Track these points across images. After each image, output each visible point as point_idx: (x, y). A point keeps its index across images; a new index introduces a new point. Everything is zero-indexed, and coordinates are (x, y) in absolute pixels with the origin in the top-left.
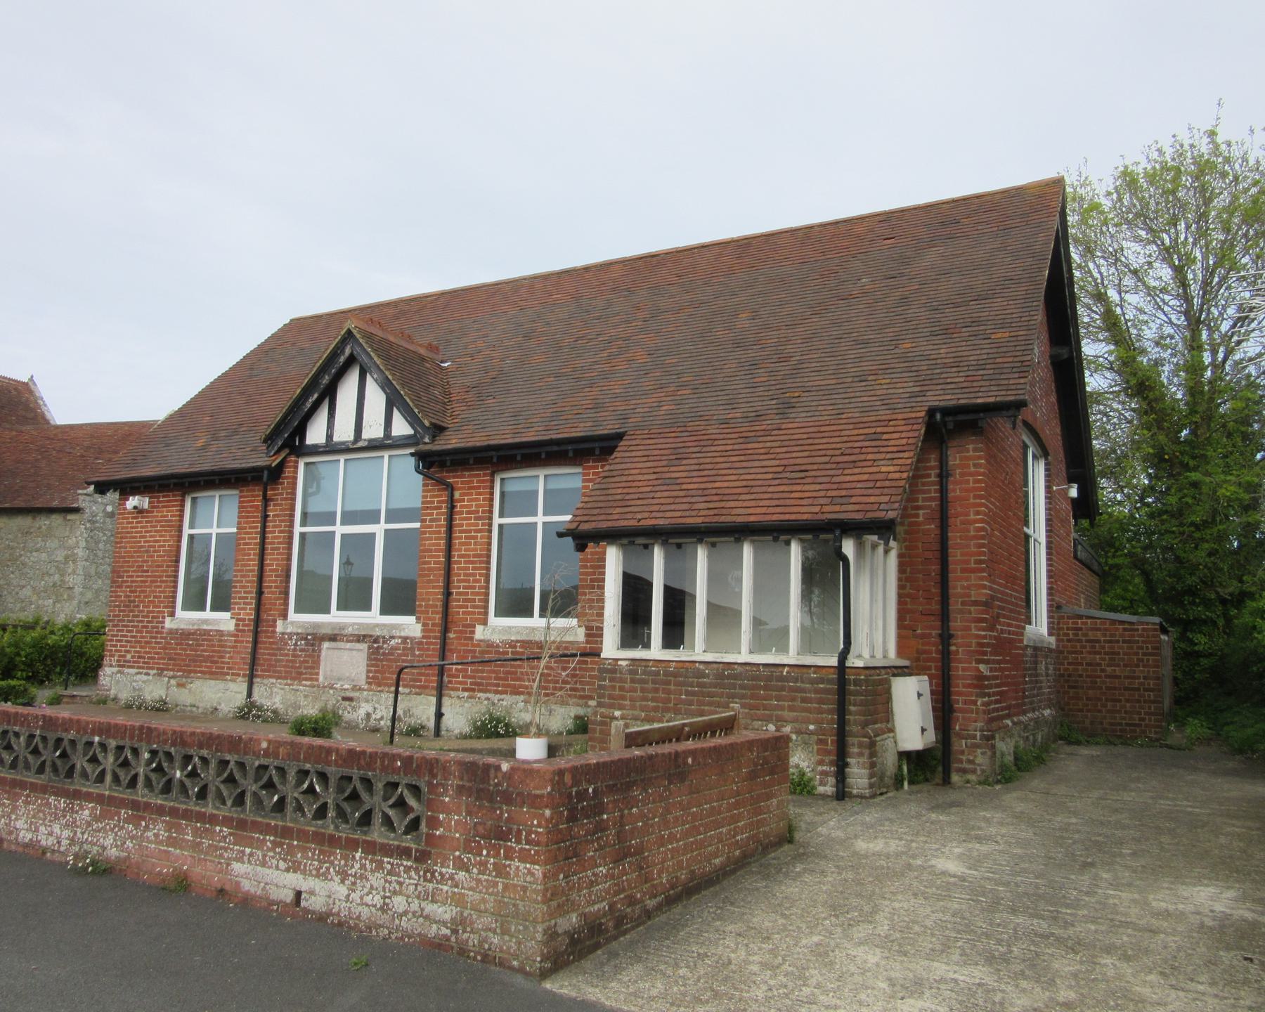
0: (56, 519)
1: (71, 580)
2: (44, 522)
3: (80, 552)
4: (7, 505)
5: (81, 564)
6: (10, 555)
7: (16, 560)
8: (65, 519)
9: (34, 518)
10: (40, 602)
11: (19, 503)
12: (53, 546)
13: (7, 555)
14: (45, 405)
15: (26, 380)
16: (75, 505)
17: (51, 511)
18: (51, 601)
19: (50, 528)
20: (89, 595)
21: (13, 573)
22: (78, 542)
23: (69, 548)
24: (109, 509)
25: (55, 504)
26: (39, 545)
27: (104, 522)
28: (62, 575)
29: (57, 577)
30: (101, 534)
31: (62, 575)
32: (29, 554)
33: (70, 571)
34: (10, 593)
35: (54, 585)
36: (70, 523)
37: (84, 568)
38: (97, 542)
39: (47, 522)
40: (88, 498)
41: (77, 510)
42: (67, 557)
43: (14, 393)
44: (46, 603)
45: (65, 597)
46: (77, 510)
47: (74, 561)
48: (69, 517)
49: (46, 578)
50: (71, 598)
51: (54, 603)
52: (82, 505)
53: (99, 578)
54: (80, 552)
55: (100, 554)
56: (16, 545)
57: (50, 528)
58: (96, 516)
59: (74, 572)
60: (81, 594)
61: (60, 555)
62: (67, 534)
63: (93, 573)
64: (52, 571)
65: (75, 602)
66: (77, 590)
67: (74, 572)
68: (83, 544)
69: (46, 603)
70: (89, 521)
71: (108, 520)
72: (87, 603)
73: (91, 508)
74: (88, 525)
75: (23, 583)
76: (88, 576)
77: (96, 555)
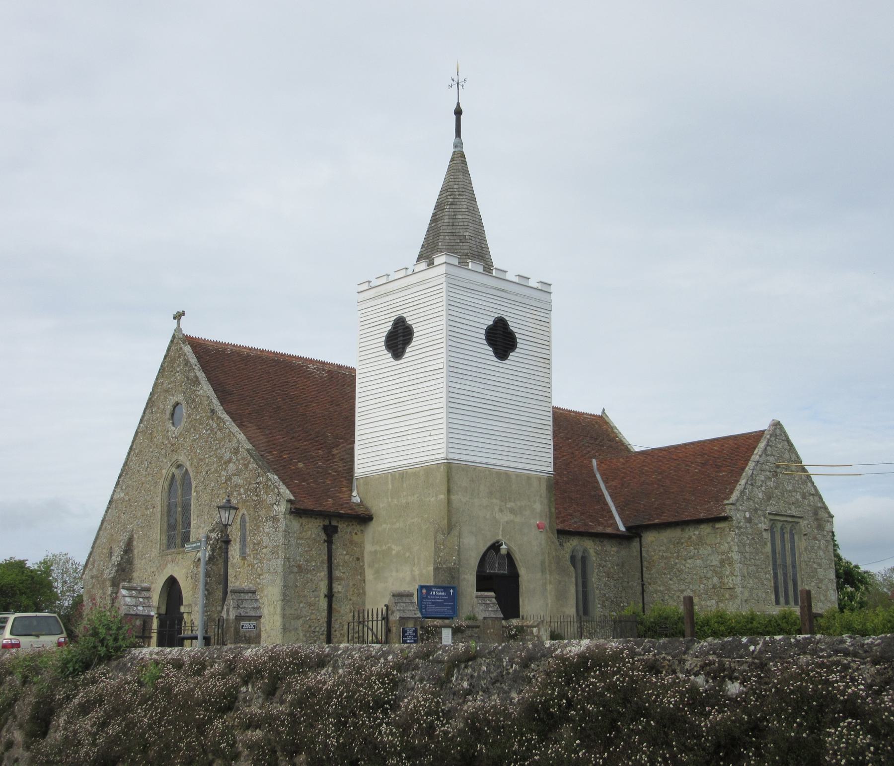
0: (705, 529)
1: (730, 582)
2: (693, 533)
3: (736, 557)
4: (656, 521)
5: (737, 566)
6: (665, 564)
7: (673, 568)
8: (714, 527)
9: (683, 530)
10: (703, 603)
11: (665, 518)
12: (706, 552)
13: (662, 565)
14: (620, 433)
15: (600, 414)
16: (723, 515)
17: (699, 522)
18: (714, 601)
19: (700, 538)
20: (746, 594)
21: (671, 580)
22: (730, 548)
23: (723, 553)
24: (747, 515)
25: (702, 516)
26: (692, 554)
27: (746, 528)
28: (721, 578)
29: (715, 580)
30: (745, 538)
31: (721, 578)
32: (683, 562)
33: (727, 573)
34: (672, 597)
35: (714, 587)
36: (718, 531)
37: (740, 570)
38: (744, 546)
39: (697, 533)
40: (733, 507)
41: (725, 519)
42: (722, 562)
43: (597, 426)
44: (709, 603)
45: (727, 596)
46: (725, 519)
47: (731, 564)
48: (718, 525)
49: (705, 582)
50: (733, 597)
51: (717, 603)
52: (732, 513)
53: (750, 577)
54: (736, 557)
55: (747, 555)
56: (669, 555)
57: (700, 538)
58: (739, 523)
59: (732, 574)
60: (742, 593)
61: (715, 561)
62: (718, 540)
63: (746, 573)
64: (709, 575)
65: (738, 601)
66: (739, 590)
67: (732, 574)
68: (735, 548)
69: (709, 603)
70: (737, 527)
71: (748, 525)
72: (746, 601)
73: (736, 516)
74: (737, 531)
75: (683, 587)
76: (743, 576)
77: (745, 557)
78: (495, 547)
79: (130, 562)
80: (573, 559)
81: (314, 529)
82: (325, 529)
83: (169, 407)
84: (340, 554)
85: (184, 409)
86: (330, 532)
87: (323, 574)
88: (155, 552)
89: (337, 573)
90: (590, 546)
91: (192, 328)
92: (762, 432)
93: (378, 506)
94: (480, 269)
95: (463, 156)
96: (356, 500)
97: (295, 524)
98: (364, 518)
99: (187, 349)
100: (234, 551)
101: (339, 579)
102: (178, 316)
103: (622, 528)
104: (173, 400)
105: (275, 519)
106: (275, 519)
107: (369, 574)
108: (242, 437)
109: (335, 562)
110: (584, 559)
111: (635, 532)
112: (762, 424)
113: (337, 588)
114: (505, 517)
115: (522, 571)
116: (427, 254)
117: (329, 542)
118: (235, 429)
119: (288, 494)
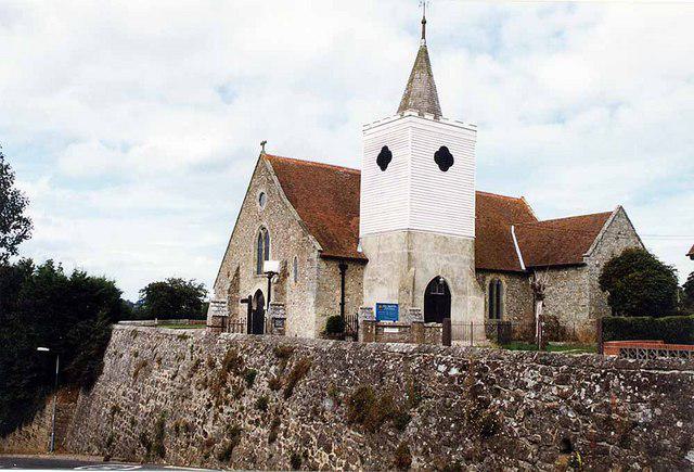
2: (564, 273)
17: (566, 267)
78: (437, 279)
79: (238, 279)
80: (491, 285)
81: (334, 267)
82: (340, 267)
83: (258, 196)
84: (349, 283)
85: (266, 195)
86: (343, 269)
87: (339, 292)
88: (250, 276)
89: (347, 292)
90: (503, 279)
91: (270, 150)
92: (610, 214)
93: (371, 254)
94: (432, 118)
95: (426, 52)
96: (359, 250)
97: (323, 265)
98: (363, 262)
99: (268, 163)
100: (291, 278)
101: (349, 295)
102: (263, 144)
103: (523, 268)
104: (260, 191)
105: (311, 261)
106: (311, 261)
107: (366, 292)
108: (296, 215)
109: (346, 285)
110: (498, 286)
111: (530, 271)
112: (612, 208)
113: (347, 299)
114: (445, 262)
115: (452, 293)
116: (403, 108)
117: (343, 274)
118: (292, 209)
119: (319, 248)
